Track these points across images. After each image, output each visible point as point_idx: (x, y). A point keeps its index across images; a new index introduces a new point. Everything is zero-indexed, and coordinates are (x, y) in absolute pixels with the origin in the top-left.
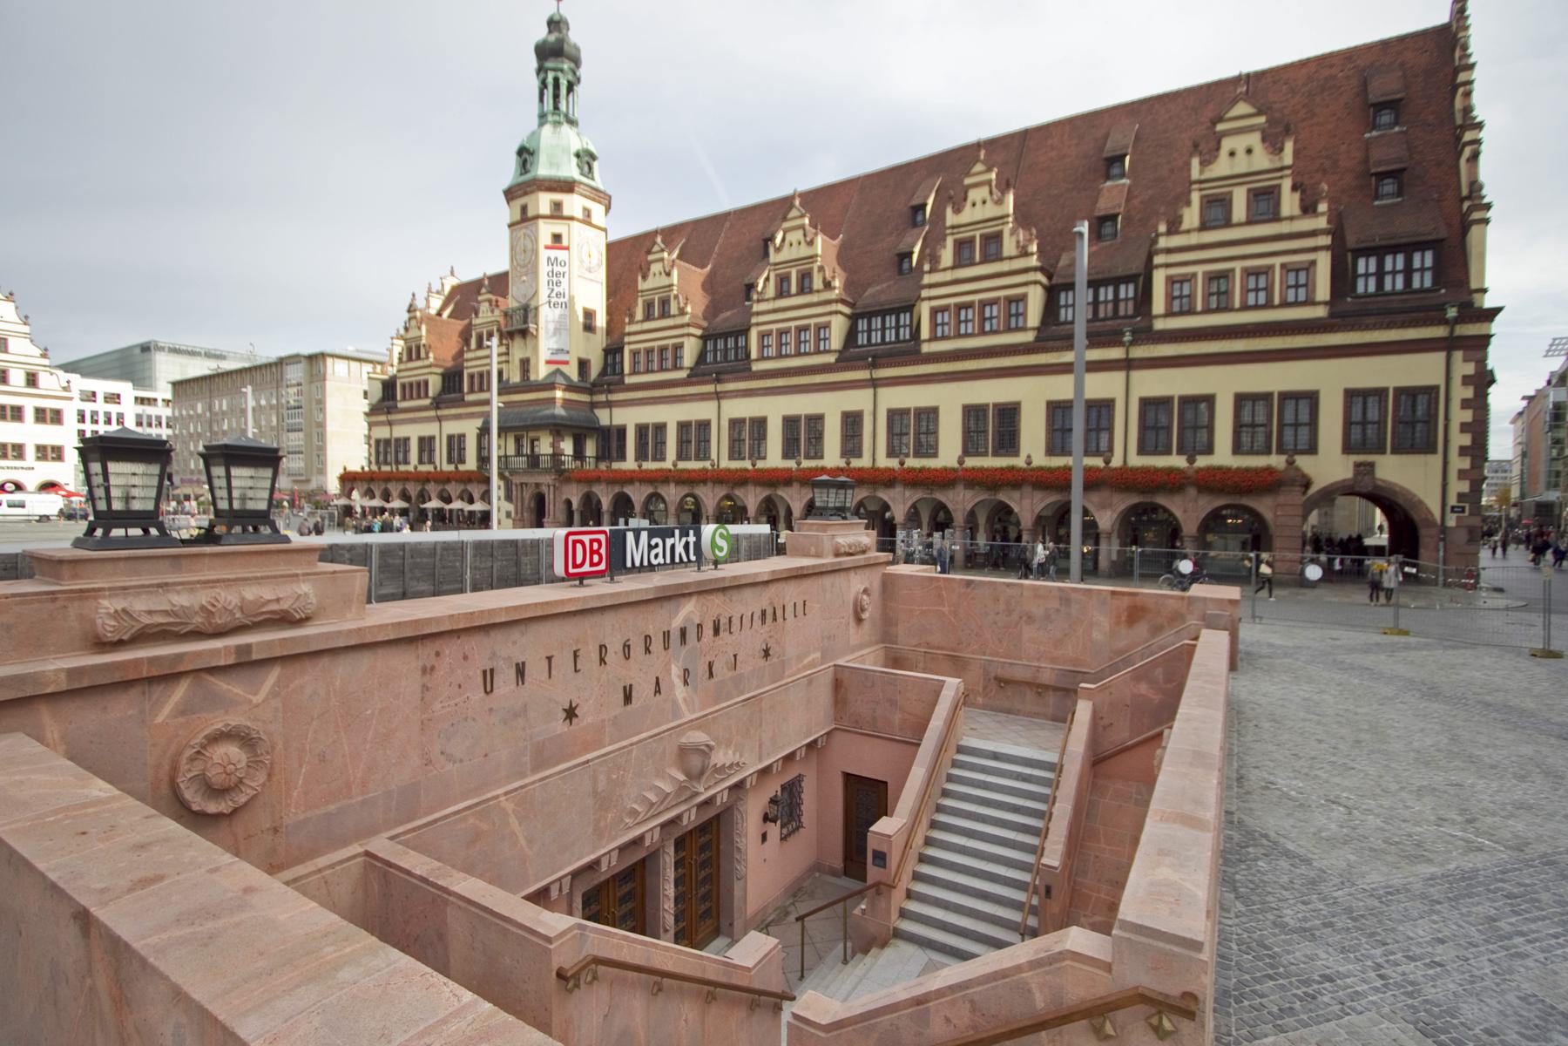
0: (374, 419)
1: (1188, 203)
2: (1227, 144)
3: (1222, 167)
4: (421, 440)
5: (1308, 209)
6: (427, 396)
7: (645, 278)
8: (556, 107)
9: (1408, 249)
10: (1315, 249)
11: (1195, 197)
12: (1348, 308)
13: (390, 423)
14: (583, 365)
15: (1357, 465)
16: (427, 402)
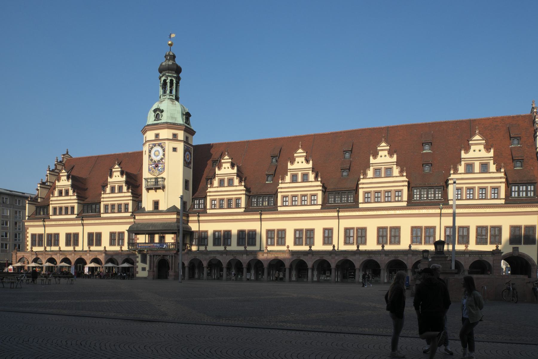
0: (32, 224)
1: (461, 165)
2: (473, 148)
3: (471, 154)
4: (68, 236)
5: (498, 170)
6: (73, 213)
7: (219, 169)
8: (171, 92)
9: (527, 184)
10: (501, 182)
11: (463, 163)
12: (510, 201)
13: (44, 226)
14: (184, 204)
15: (513, 248)
16: (74, 216)
